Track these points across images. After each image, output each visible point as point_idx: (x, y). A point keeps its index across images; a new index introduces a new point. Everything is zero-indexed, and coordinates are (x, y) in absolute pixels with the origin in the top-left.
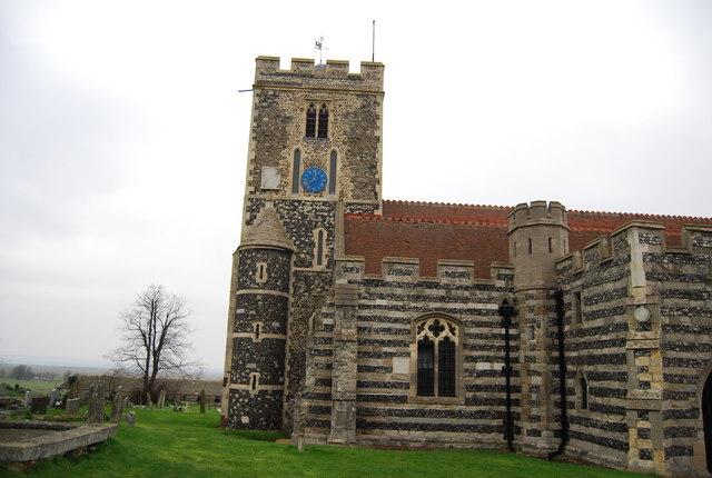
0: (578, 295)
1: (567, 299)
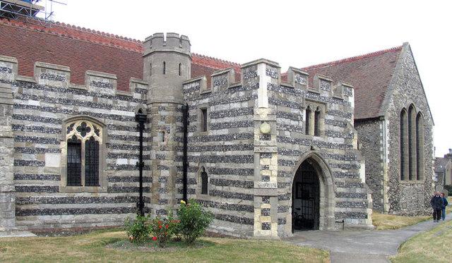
0: (204, 111)
1: (192, 113)
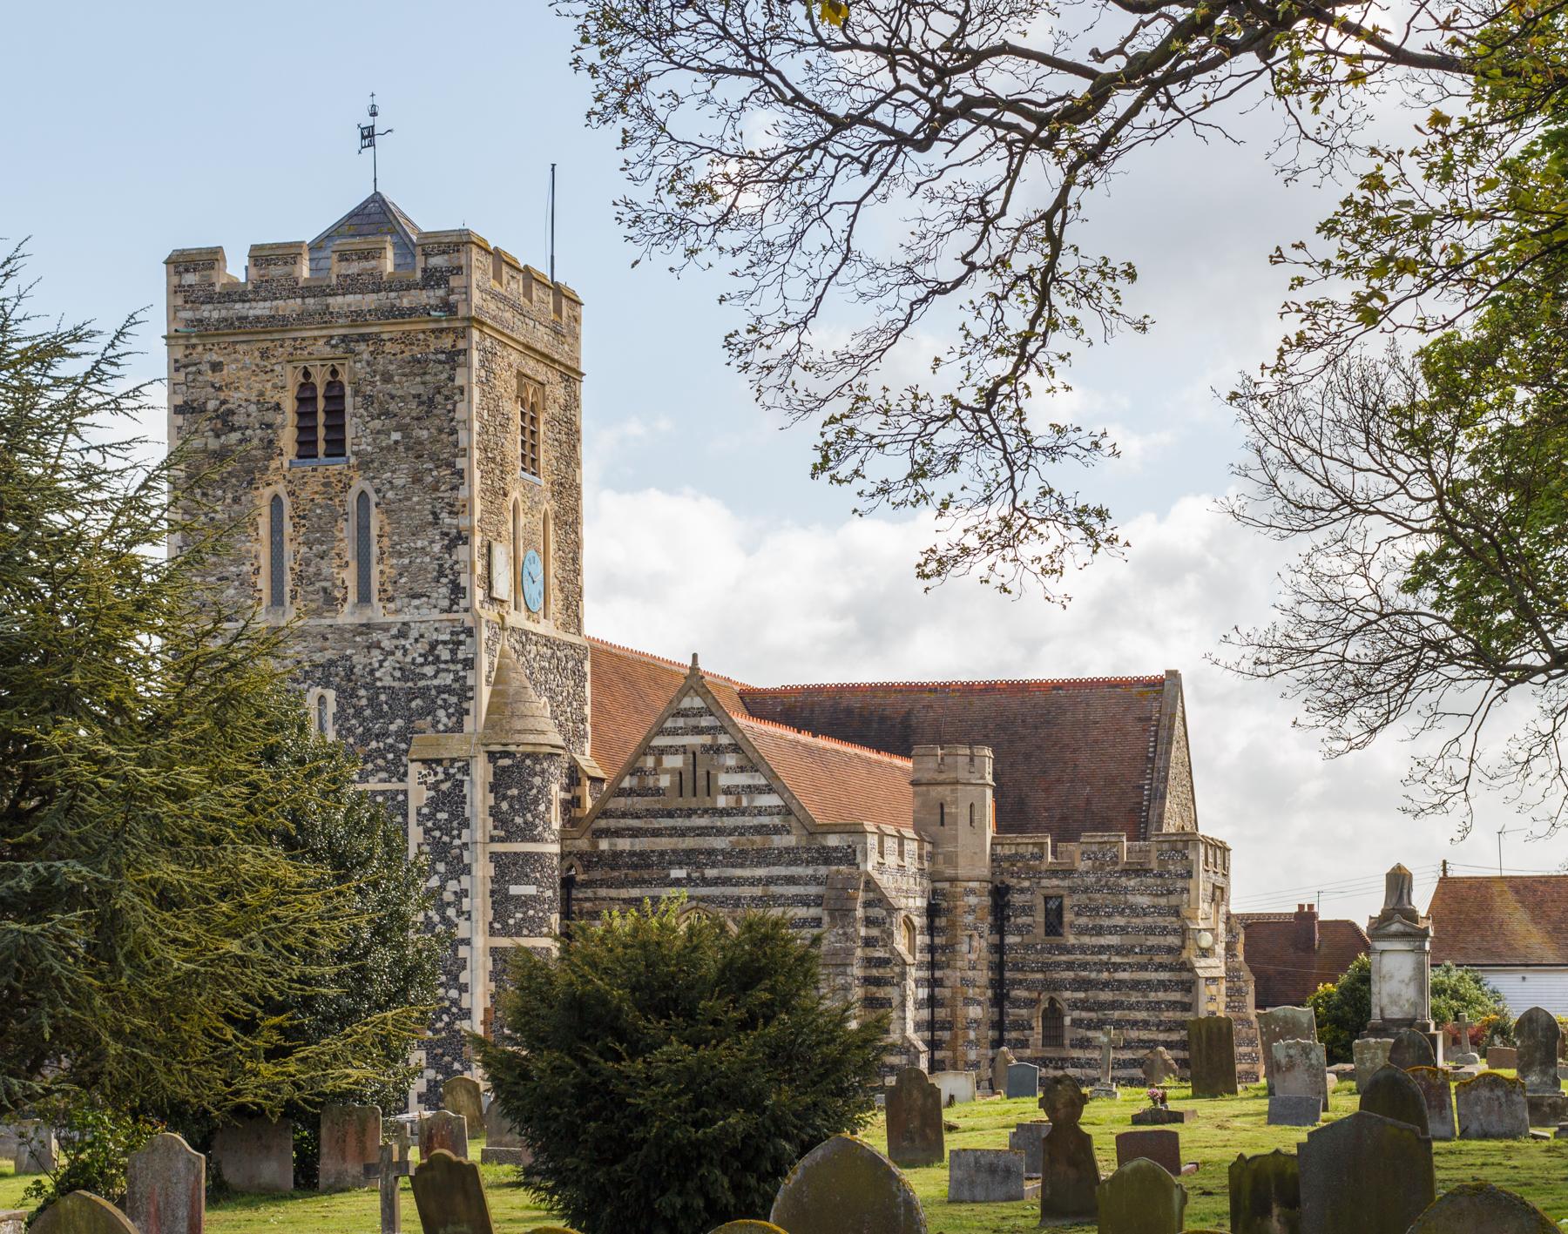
1: (1017, 899)
